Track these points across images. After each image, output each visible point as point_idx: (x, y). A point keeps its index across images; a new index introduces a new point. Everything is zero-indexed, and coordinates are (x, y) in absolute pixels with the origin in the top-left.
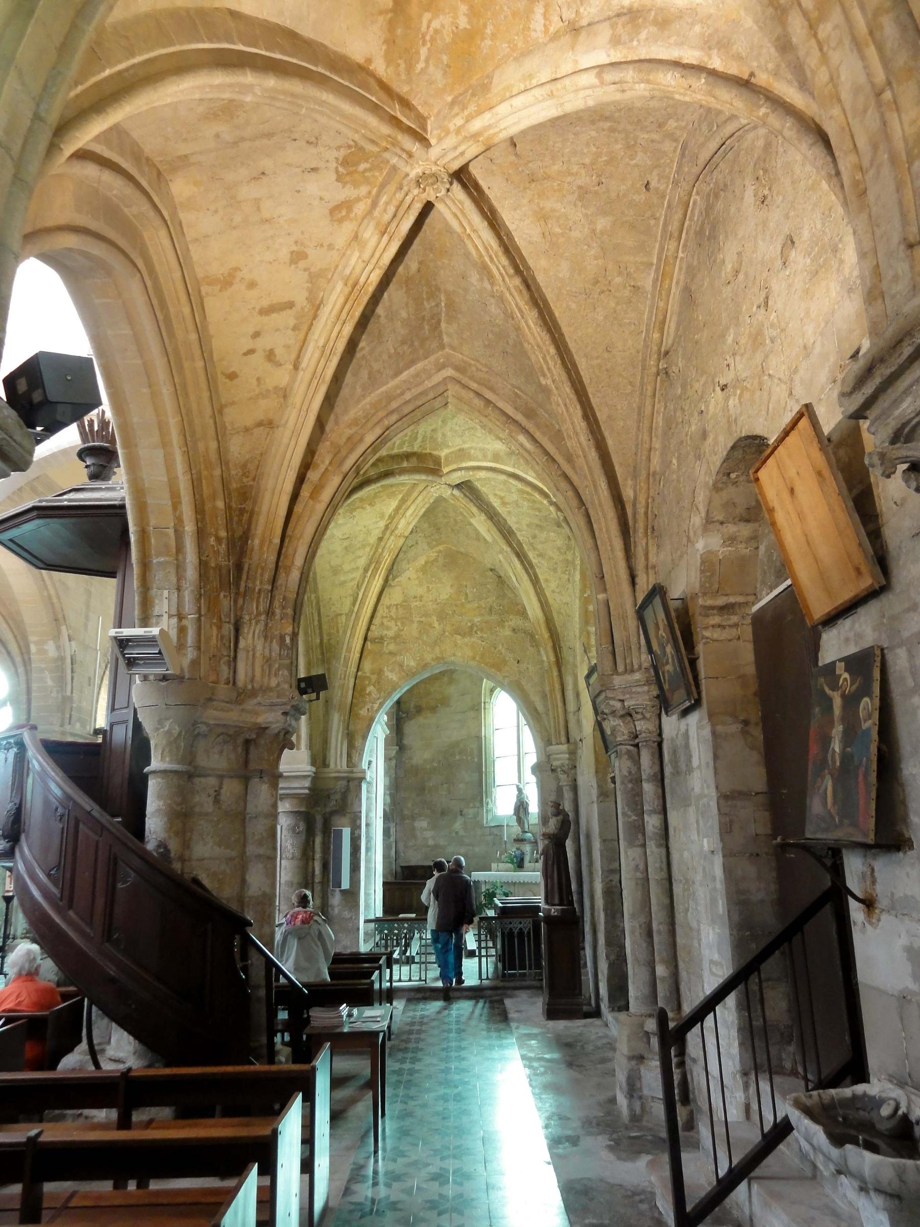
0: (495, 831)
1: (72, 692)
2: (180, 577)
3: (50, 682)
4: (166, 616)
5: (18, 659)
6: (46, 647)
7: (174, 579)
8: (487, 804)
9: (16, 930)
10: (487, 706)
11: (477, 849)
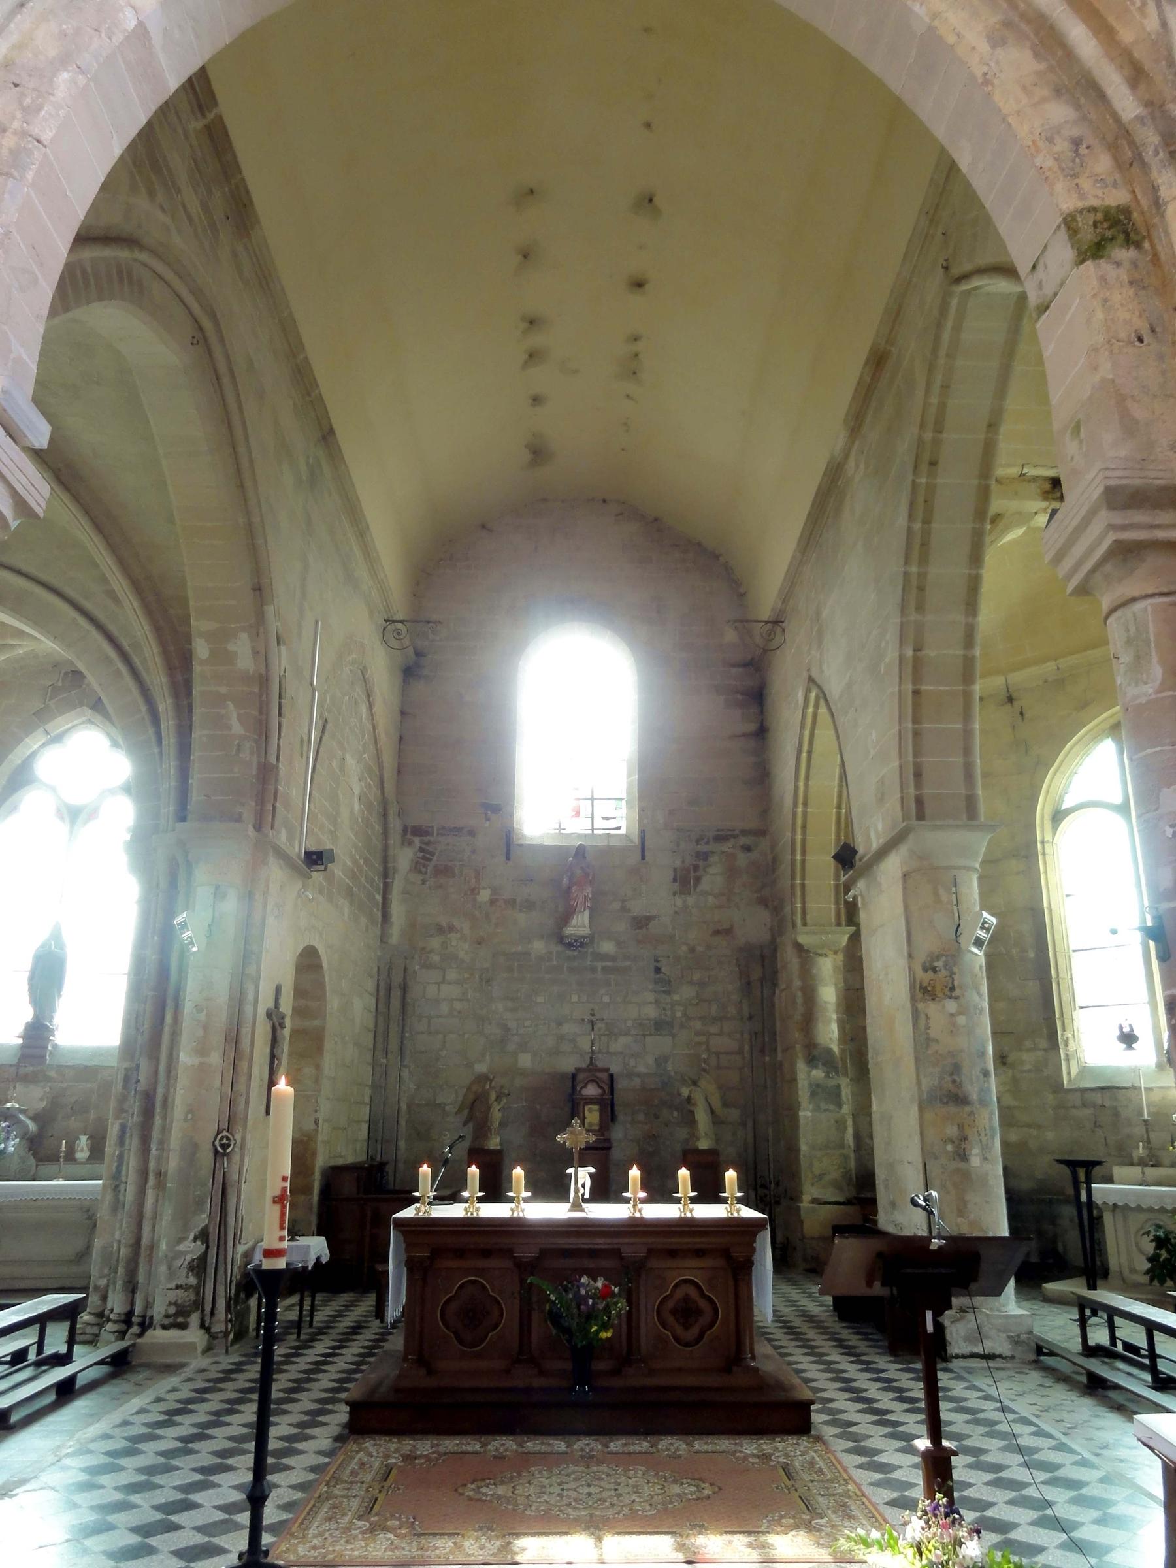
0: (1098, 1098)
1: (278, 760)
3: (237, 728)
5: (158, 679)
6: (231, 647)
8: (1066, 1044)
9: (148, 1305)
10: (1048, 851)
11: (1050, 1135)
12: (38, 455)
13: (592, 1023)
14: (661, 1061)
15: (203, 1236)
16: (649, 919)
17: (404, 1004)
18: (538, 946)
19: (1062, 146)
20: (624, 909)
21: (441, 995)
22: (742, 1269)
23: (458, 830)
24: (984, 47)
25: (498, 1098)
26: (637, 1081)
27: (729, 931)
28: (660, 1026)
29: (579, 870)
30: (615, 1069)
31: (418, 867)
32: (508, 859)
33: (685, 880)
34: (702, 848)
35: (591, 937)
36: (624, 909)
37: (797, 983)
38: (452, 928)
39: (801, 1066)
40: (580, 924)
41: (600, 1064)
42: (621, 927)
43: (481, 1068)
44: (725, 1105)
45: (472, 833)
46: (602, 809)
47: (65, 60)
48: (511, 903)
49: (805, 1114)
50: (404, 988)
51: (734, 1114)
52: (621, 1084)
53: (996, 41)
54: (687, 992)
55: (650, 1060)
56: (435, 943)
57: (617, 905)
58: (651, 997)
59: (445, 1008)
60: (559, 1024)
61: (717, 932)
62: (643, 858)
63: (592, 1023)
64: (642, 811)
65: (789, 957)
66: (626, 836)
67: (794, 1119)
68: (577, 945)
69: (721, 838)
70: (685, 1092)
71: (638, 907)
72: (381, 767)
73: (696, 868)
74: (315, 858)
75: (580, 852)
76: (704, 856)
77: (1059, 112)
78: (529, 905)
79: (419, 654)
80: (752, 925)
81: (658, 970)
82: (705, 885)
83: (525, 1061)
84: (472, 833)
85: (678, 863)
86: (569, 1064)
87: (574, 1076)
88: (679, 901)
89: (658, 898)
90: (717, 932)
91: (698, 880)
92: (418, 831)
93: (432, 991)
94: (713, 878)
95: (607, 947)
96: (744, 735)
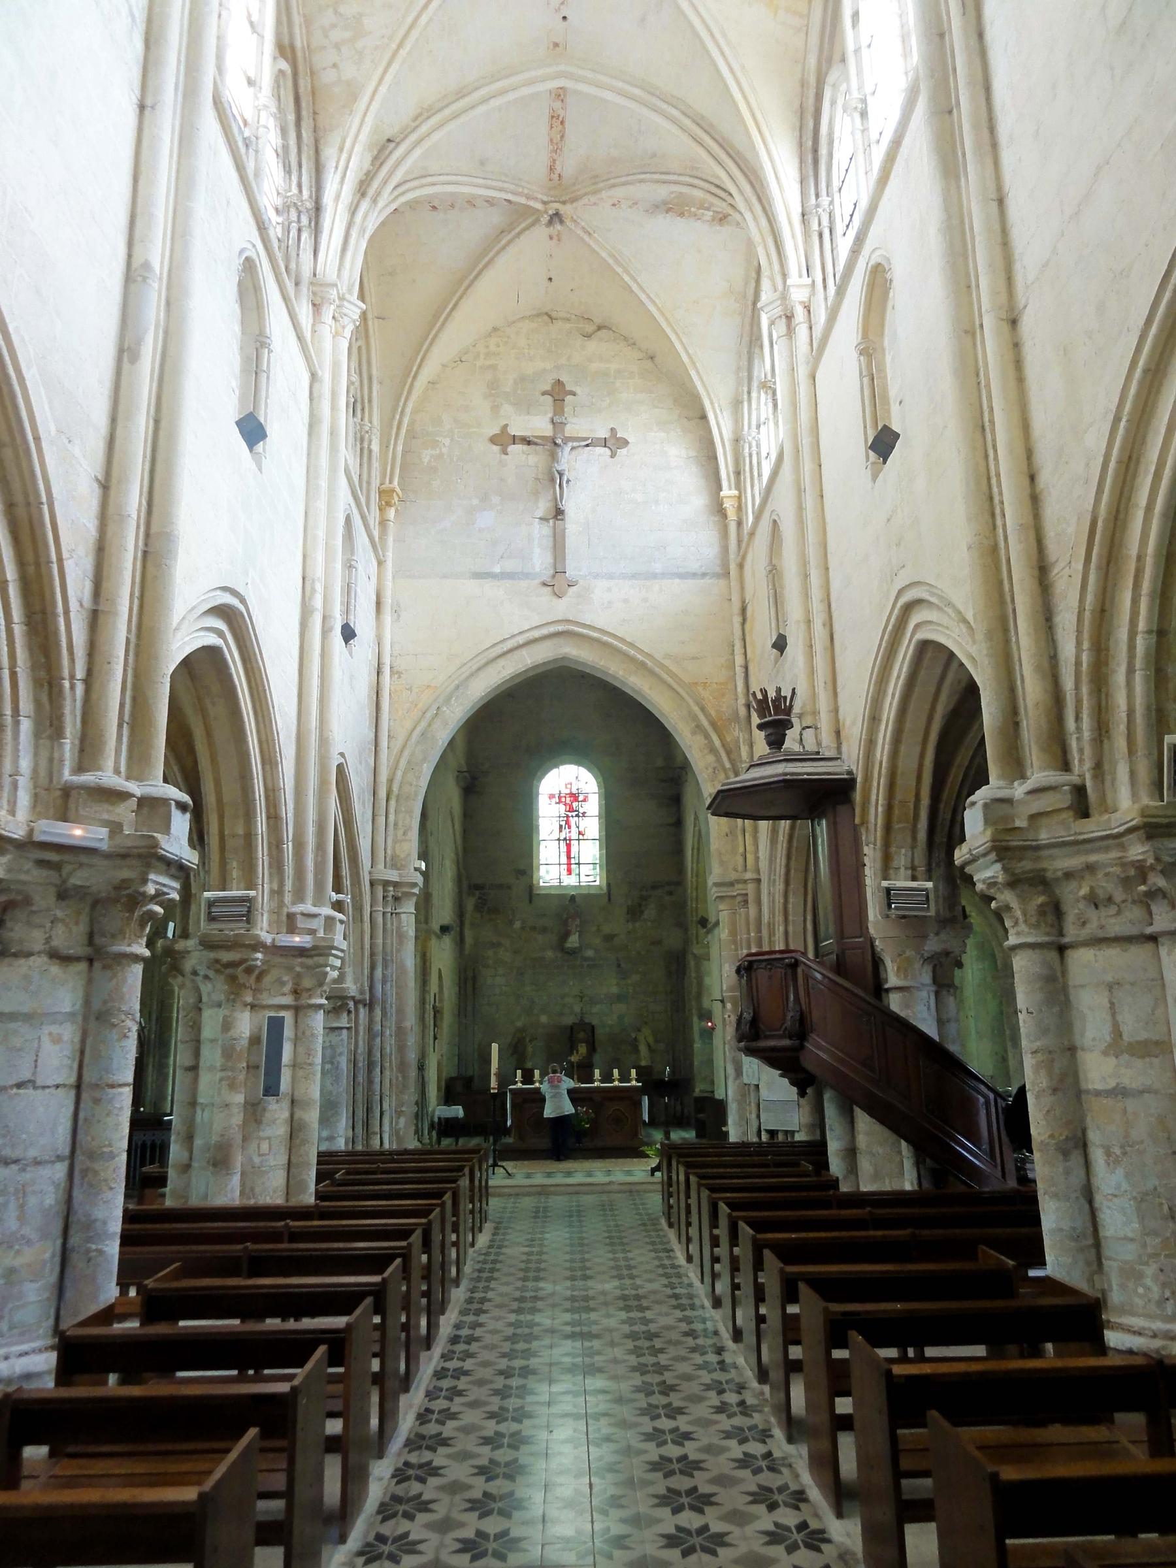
2: (914, 838)
4: (902, 870)
7: (909, 840)
12: (422, 873)
13: (581, 998)
14: (621, 1018)
15: (417, 1103)
16: (615, 935)
17: (474, 989)
18: (550, 954)
19: (710, 770)
20: (599, 930)
21: (496, 982)
22: (639, 1104)
23: (500, 886)
24: (689, 735)
25: (531, 1041)
26: (607, 1029)
27: (658, 943)
28: (620, 998)
29: (571, 906)
30: (594, 1023)
31: (478, 908)
32: (530, 902)
33: (634, 912)
34: (644, 893)
35: (580, 949)
36: (599, 930)
37: (693, 975)
38: (499, 945)
39: (695, 1019)
40: (573, 941)
41: (587, 1021)
42: (597, 941)
43: (519, 1024)
44: (656, 1041)
45: (509, 887)
46: (585, 870)
47: (425, 760)
48: (534, 928)
49: (697, 1045)
50: (474, 979)
51: (662, 1046)
52: (598, 1031)
53: (694, 733)
54: (635, 978)
55: (615, 1017)
56: (490, 953)
57: (594, 929)
58: (614, 982)
59: (497, 991)
60: (563, 997)
61: (653, 943)
62: (609, 899)
63: (581, 998)
64: (608, 871)
65: (690, 957)
66: (599, 887)
67: (692, 1046)
68: (572, 952)
69: (654, 887)
70: (633, 1035)
71: (607, 929)
72: (457, 854)
73: (640, 905)
74: (444, 929)
75: (573, 898)
76: (644, 898)
77: (711, 758)
78: (544, 930)
79: (474, 778)
80: (673, 940)
81: (619, 966)
82: (646, 915)
83: (544, 1019)
84: (509, 887)
85: (630, 903)
86: (569, 1020)
87: (572, 1028)
88: (630, 926)
89: (617, 925)
90: (653, 943)
91: (642, 912)
92: (478, 887)
93: (489, 981)
94: (650, 912)
95: (590, 953)
96: (669, 825)
